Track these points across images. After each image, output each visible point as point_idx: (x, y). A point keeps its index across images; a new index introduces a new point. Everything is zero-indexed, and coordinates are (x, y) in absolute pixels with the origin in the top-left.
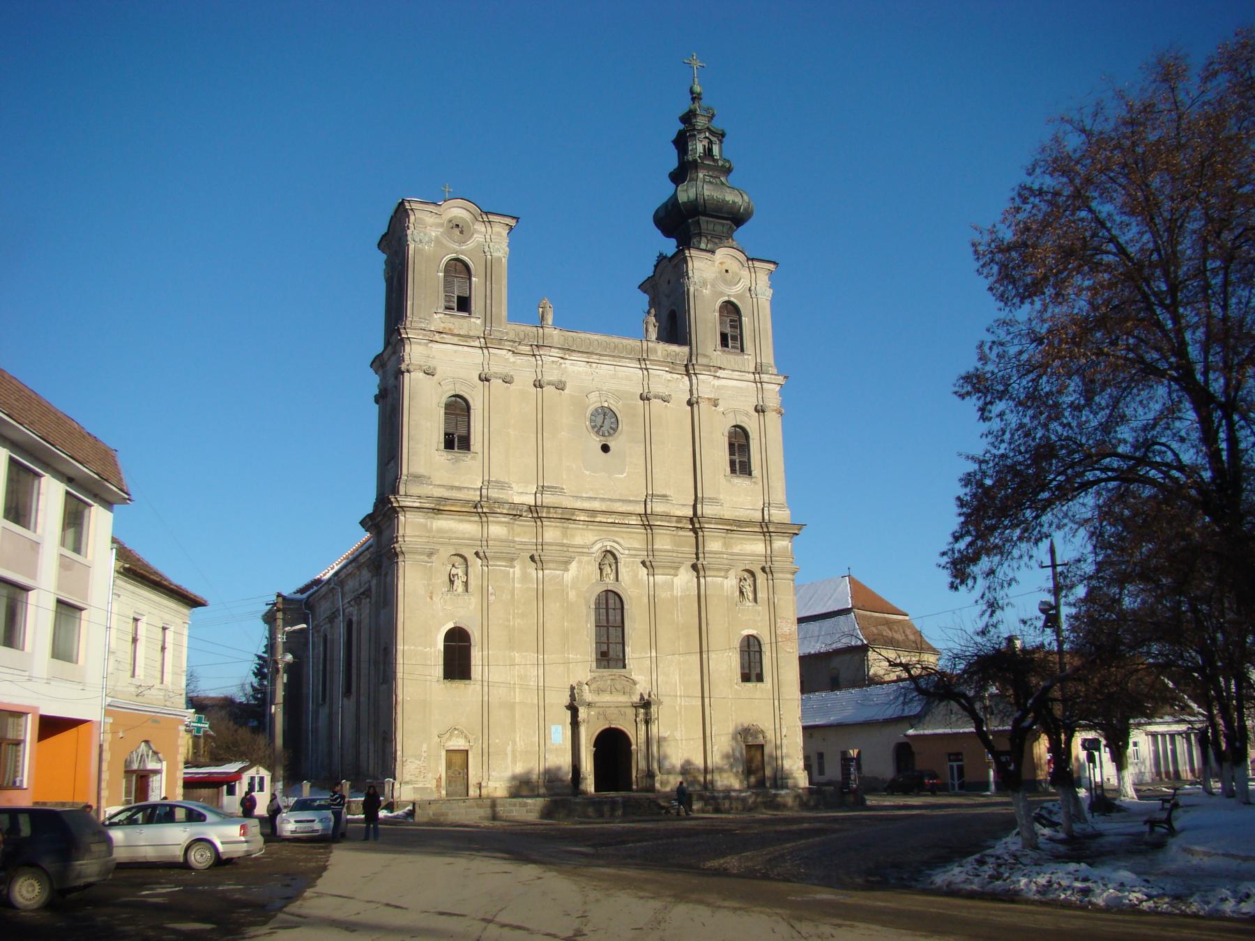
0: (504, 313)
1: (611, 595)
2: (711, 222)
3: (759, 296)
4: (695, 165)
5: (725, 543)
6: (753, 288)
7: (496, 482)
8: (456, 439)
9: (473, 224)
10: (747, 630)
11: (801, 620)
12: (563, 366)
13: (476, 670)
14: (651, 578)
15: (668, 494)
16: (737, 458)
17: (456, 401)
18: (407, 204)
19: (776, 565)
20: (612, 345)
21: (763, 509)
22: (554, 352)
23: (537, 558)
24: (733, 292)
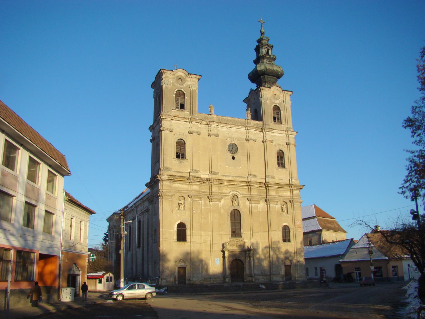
0: (197, 110)
1: (236, 211)
2: (269, 77)
3: (287, 104)
4: (263, 57)
5: (276, 192)
6: (284, 101)
7: (195, 170)
8: (180, 155)
9: (186, 78)
11: (304, 219)
12: (218, 128)
13: (188, 237)
14: (250, 205)
15: (256, 174)
16: (280, 162)
17: (180, 141)
18: (162, 71)
19: (295, 200)
20: (235, 121)
21: (290, 180)
22: (215, 123)
23: (210, 197)
24: (277, 102)
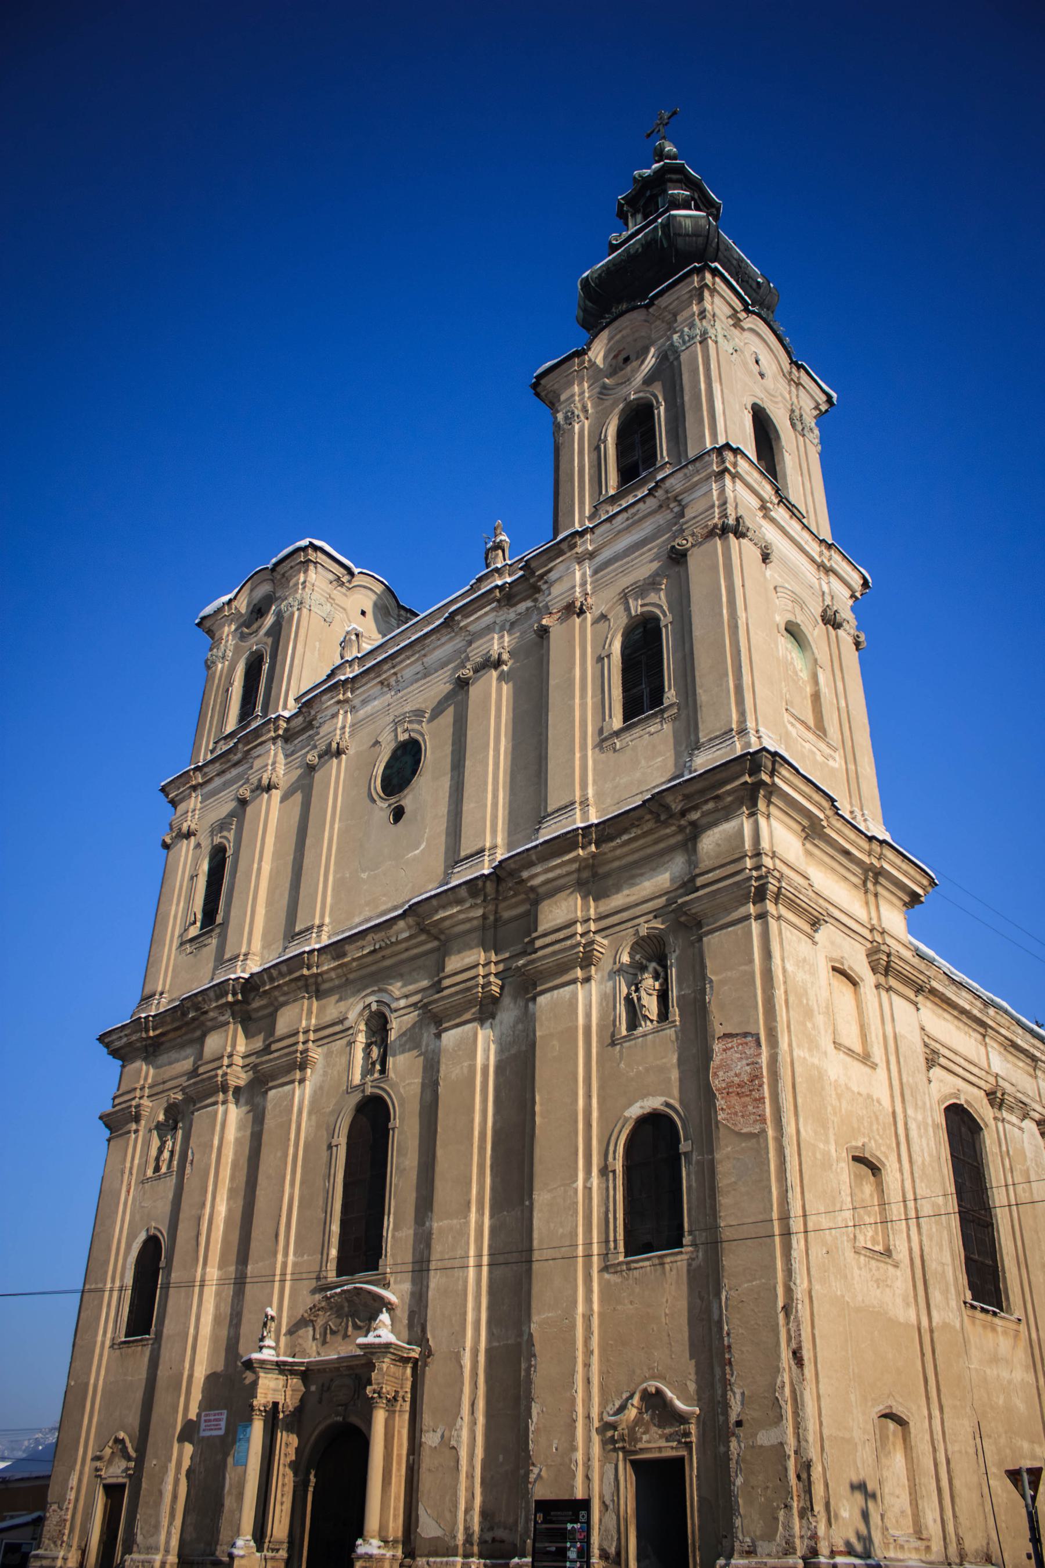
10: (638, 1104)
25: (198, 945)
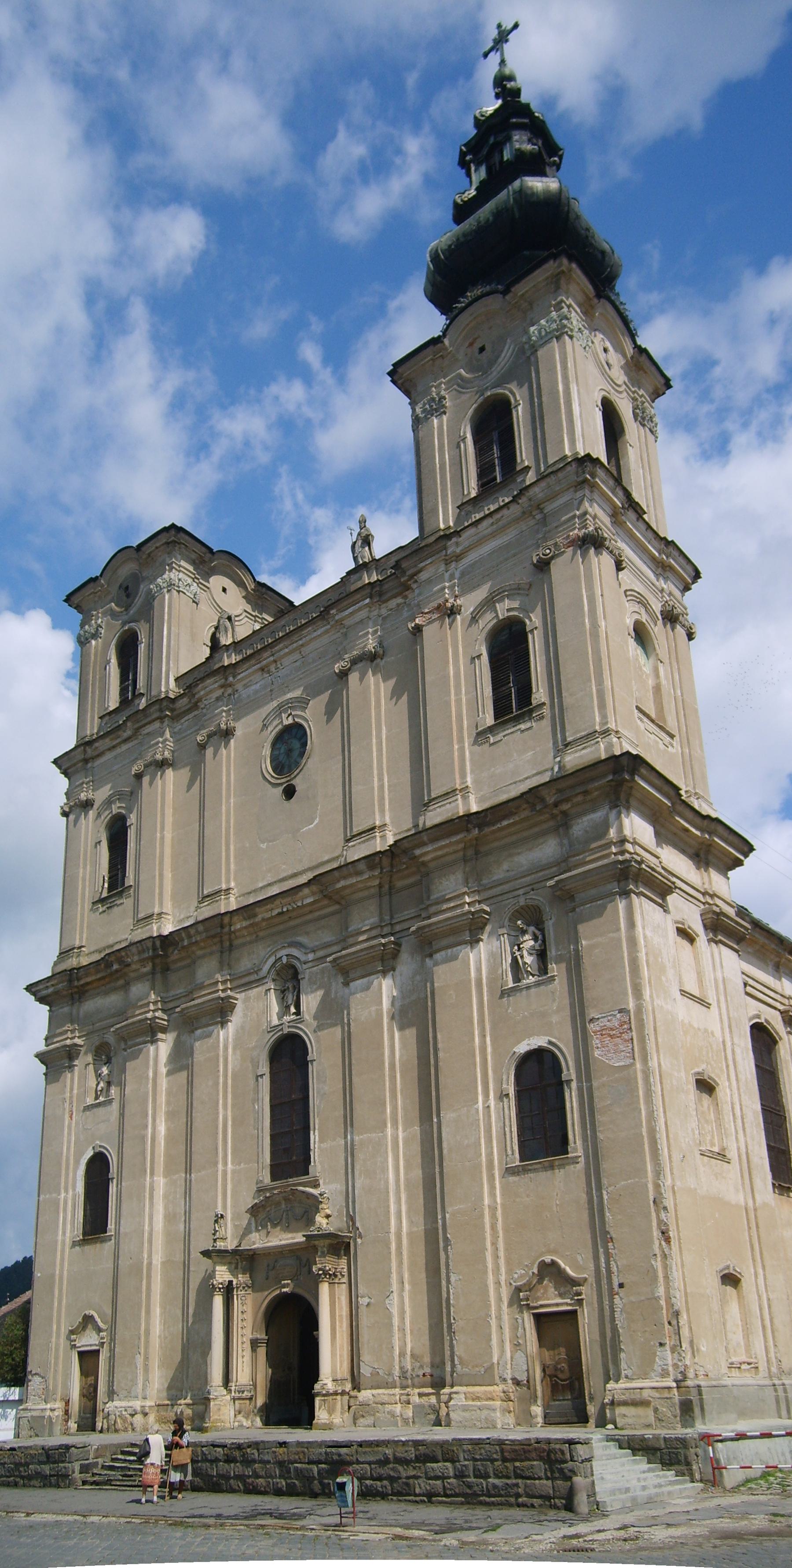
10: (526, 1042)
25: (108, 905)
